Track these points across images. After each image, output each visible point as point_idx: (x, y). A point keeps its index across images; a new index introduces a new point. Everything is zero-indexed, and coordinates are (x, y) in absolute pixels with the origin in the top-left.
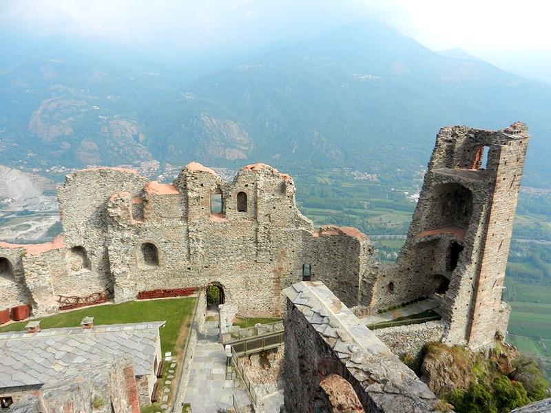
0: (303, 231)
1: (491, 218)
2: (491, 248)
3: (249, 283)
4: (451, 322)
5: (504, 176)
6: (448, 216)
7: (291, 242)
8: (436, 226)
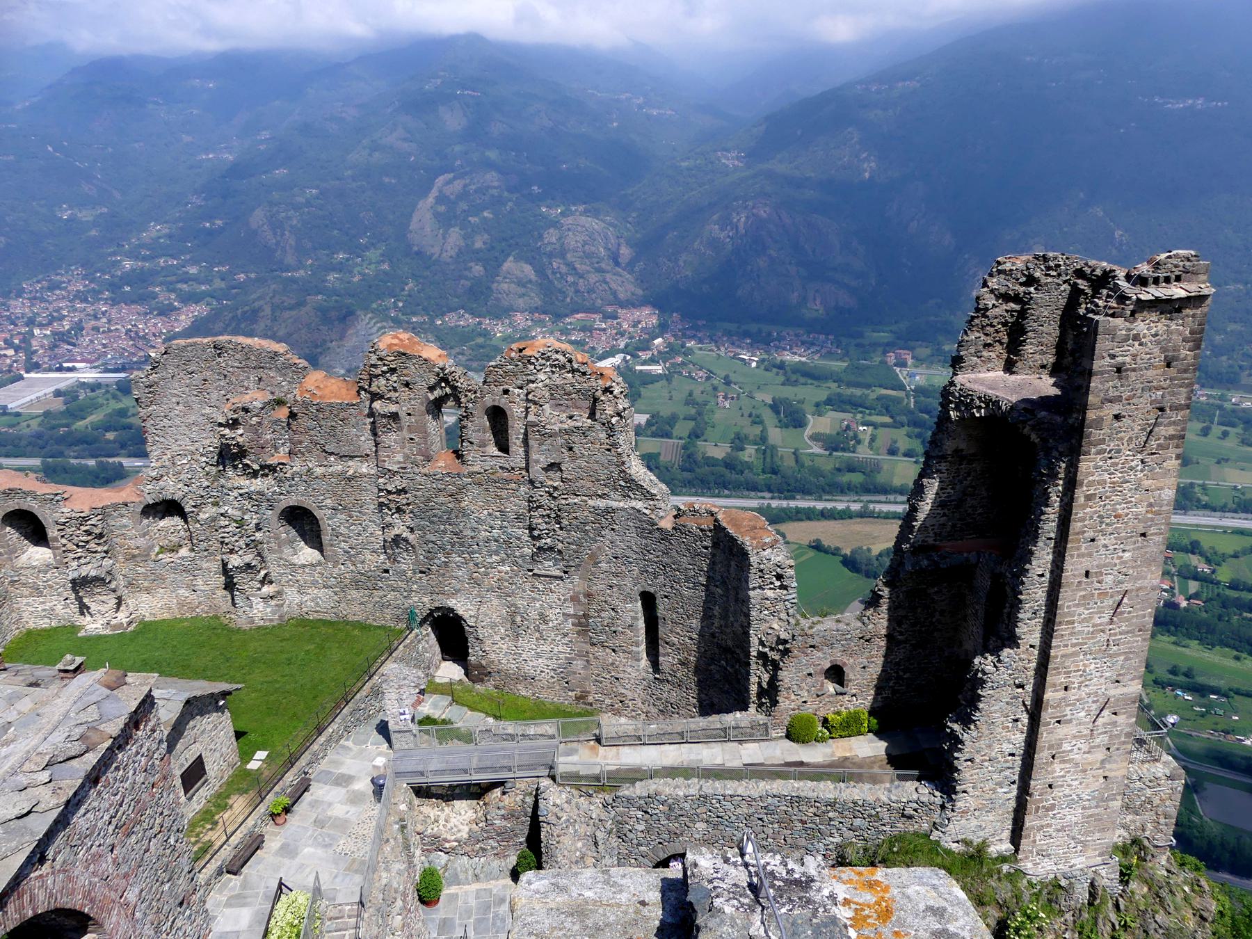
0: (639, 511)
1: (1075, 526)
2: (1081, 609)
3: (518, 619)
5: (1116, 408)
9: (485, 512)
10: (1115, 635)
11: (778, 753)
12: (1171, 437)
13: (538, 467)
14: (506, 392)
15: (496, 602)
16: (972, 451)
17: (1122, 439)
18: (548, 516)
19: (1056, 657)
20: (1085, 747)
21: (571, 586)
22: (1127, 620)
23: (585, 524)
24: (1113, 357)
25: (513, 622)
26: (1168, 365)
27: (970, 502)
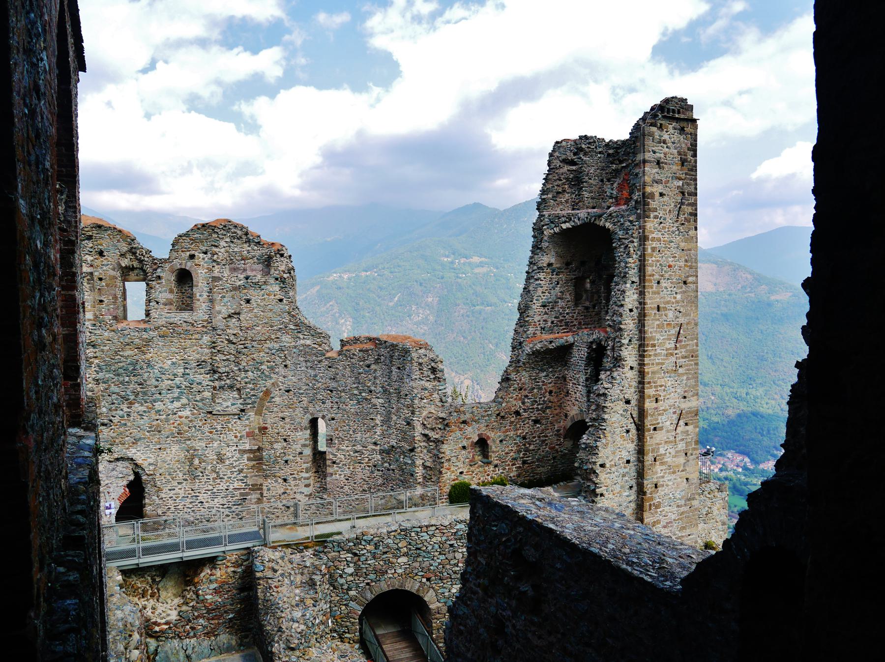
1: (649, 270)
4: (596, 495)
6: (587, 308)
7: (281, 370)
8: (568, 326)
9: (169, 362)
12: (691, 214)
13: (220, 317)
14: (192, 257)
15: (175, 448)
18: (227, 360)
19: (648, 373)
20: (673, 451)
22: (685, 346)
23: (261, 364)
24: (654, 152)
25: (191, 464)
26: (683, 165)
27: (561, 303)
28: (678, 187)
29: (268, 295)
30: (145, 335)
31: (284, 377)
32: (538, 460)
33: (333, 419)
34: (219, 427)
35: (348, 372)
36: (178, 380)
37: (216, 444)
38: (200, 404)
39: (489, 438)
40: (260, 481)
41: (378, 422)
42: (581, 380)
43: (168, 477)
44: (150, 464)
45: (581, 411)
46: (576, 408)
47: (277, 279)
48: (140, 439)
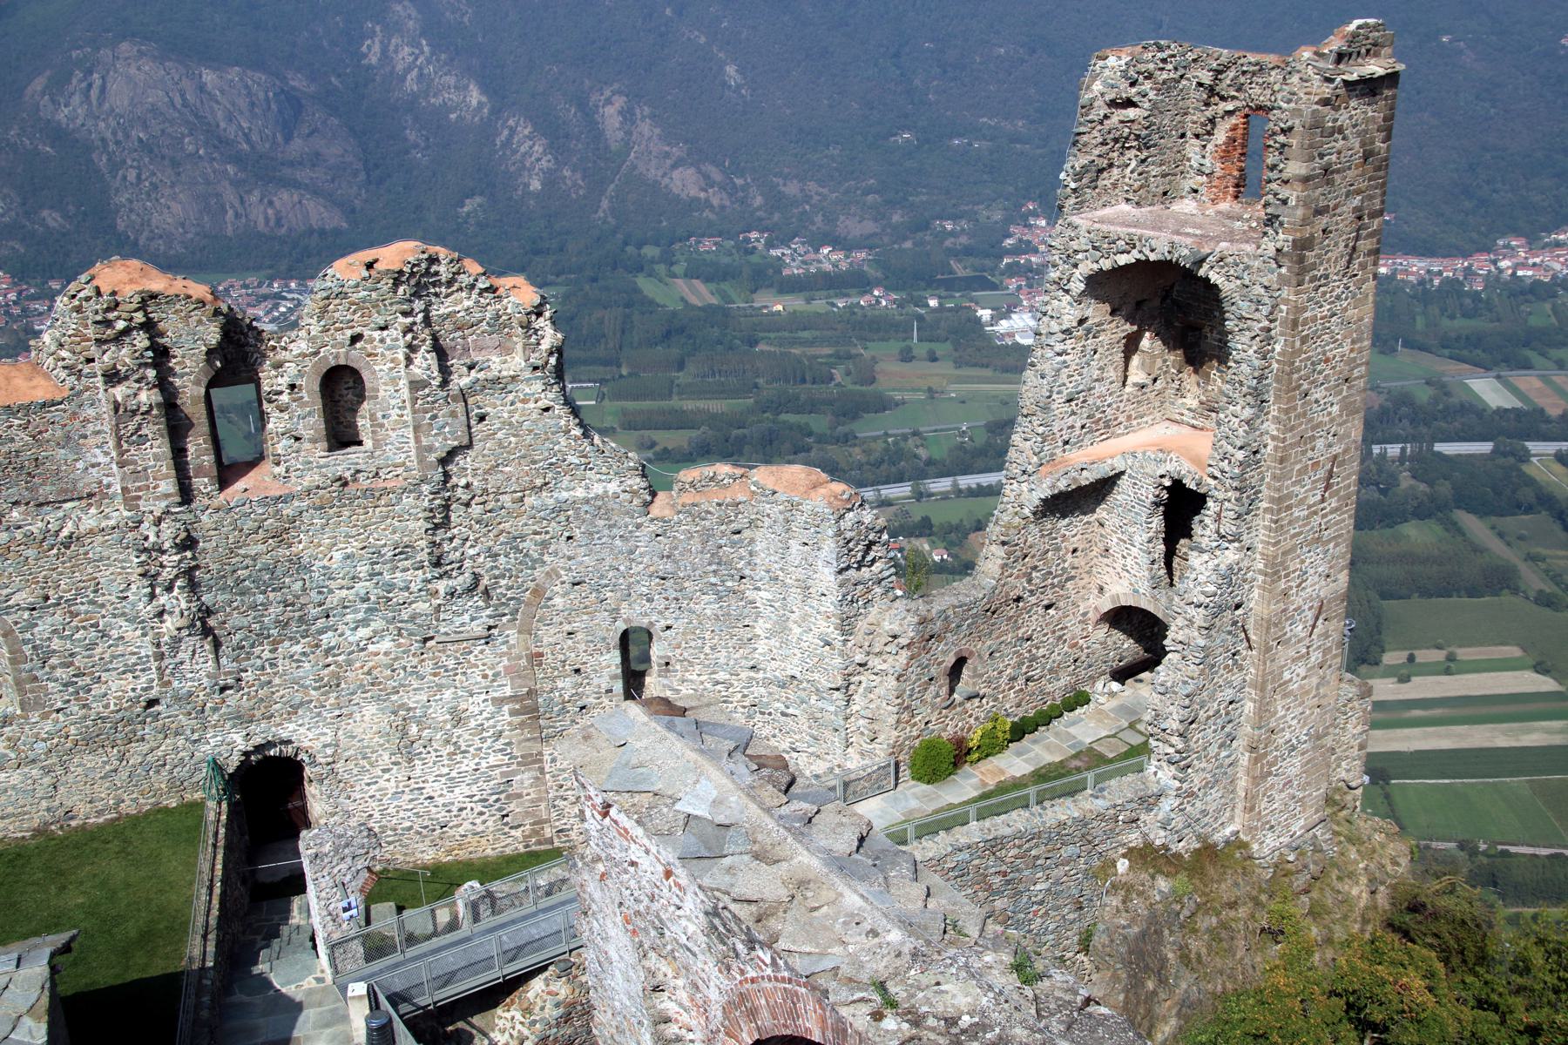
2: (1297, 489)
7: (564, 548)
10: (1324, 516)
11: (914, 804)
12: (1370, 253)
15: (371, 710)
16: (1096, 320)
17: (1329, 260)
20: (1302, 671)
21: (504, 648)
22: (1338, 491)
23: (523, 538)
25: (405, 734)
28: (1355, 209)
29: (524, 401)
30: (288, 511)
31: (570, 558)
32: (1050, 671)
33: (668, 628)
34: (451, 663)
35: (695, 545)
36: (361, 588)
37: (448, 694)
38: (409, 626)
39: (972, 653)
40: (535, 748)
41: (758, 631)
42: (1137, 539)
43: (364, 763)
44: (325, 746)
45: (1136, 591)
46: (1126, 583)
47: (536, 368)
48: (301, 704)
